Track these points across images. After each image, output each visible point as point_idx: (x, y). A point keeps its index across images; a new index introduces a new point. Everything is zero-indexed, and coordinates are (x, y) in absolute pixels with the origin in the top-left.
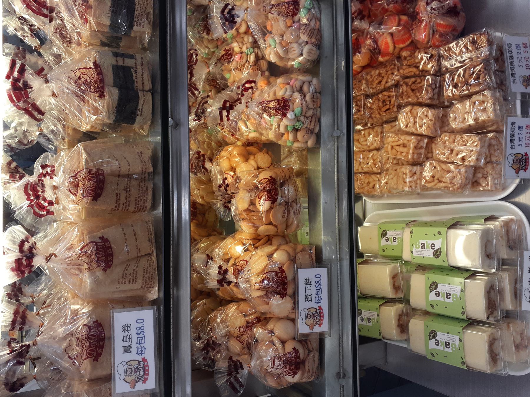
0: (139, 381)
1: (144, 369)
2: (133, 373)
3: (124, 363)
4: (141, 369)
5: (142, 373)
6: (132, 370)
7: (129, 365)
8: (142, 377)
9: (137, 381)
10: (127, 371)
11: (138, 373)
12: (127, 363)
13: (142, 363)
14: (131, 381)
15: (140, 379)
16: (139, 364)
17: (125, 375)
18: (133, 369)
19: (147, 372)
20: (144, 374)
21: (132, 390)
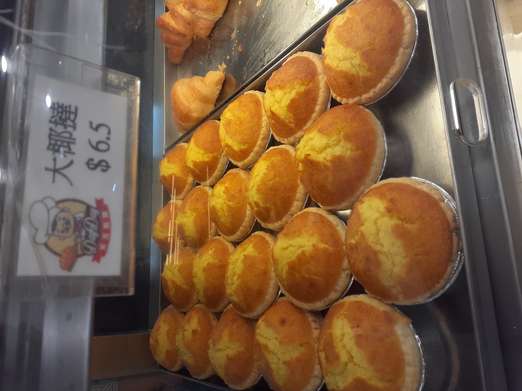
0: (84, 254)
1: (100, 226)
2: (71, 230)
3: (50, 203)
4: (92, 225)
5: (94, 235)
7: (62, 210)
9: (80, 252)
11: (83, 233)
12: (58, 202)
13: (94, 213)
14: (65, 251)
15: (88, 250)
16: (88, 212)
18: (72, 222)
19: (105, 236)
20: (98, 240)
21: (64, 273)
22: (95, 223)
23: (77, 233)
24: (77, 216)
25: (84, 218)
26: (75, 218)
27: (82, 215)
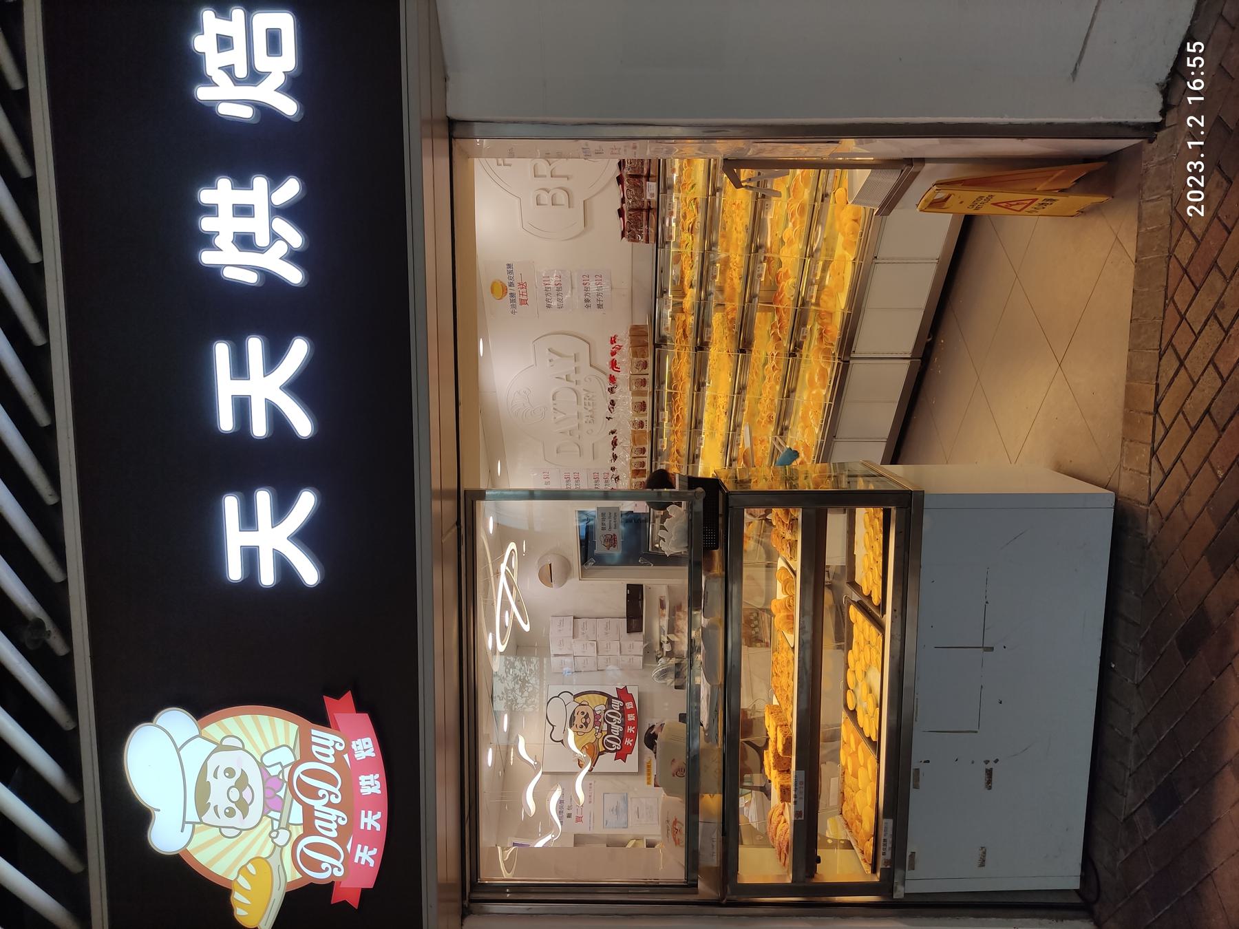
2: (256, 808)
6: (242, 783)
7: (220, 747)
8: (333, 853)
10: (203, 790)
11: (297, 814)
17: (192, 815)
18: (255, 780)
22: (330, 780)
23: (276, 815)
24: (268, 760)
25: (295, 765)
26: (262, 767)
27: (287, 757)
